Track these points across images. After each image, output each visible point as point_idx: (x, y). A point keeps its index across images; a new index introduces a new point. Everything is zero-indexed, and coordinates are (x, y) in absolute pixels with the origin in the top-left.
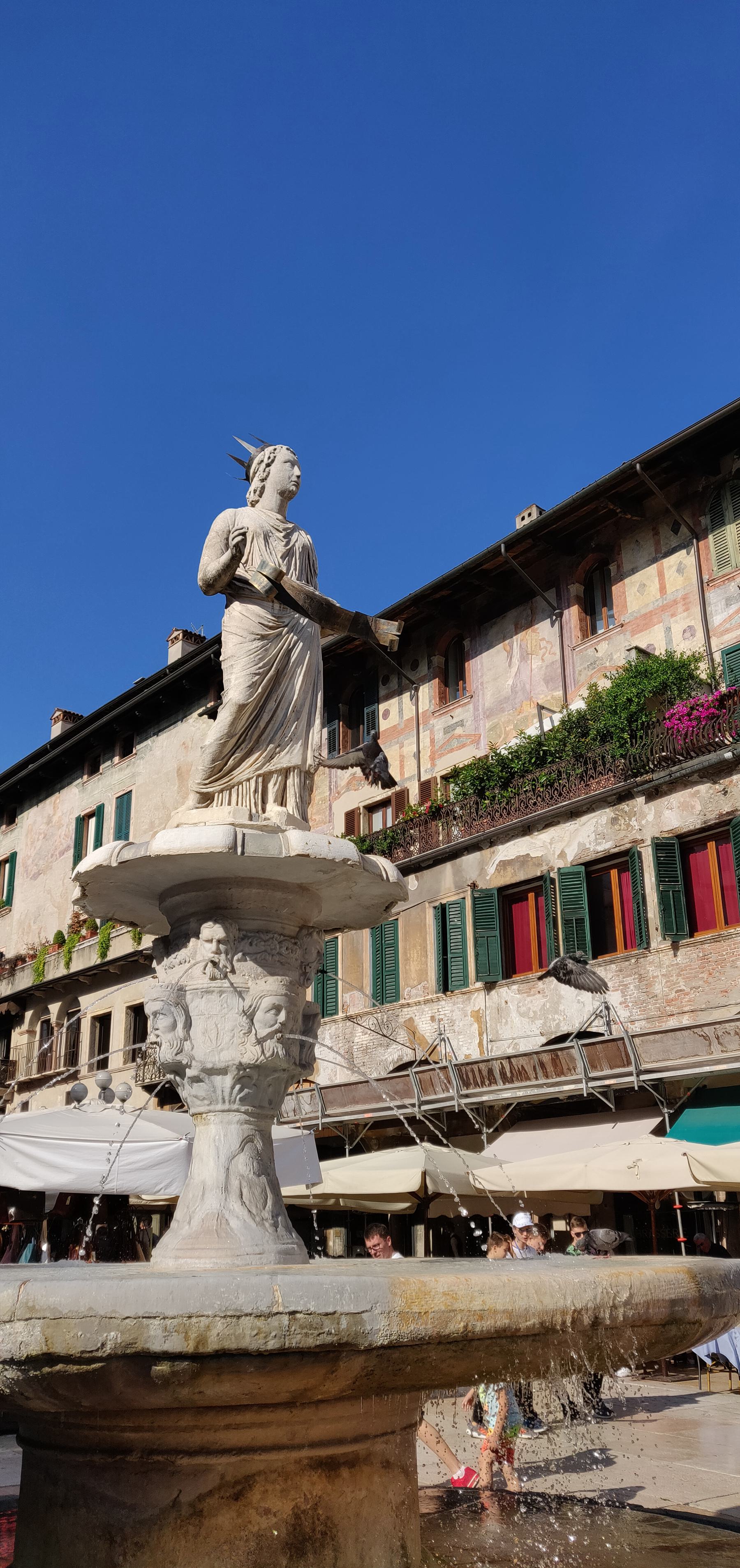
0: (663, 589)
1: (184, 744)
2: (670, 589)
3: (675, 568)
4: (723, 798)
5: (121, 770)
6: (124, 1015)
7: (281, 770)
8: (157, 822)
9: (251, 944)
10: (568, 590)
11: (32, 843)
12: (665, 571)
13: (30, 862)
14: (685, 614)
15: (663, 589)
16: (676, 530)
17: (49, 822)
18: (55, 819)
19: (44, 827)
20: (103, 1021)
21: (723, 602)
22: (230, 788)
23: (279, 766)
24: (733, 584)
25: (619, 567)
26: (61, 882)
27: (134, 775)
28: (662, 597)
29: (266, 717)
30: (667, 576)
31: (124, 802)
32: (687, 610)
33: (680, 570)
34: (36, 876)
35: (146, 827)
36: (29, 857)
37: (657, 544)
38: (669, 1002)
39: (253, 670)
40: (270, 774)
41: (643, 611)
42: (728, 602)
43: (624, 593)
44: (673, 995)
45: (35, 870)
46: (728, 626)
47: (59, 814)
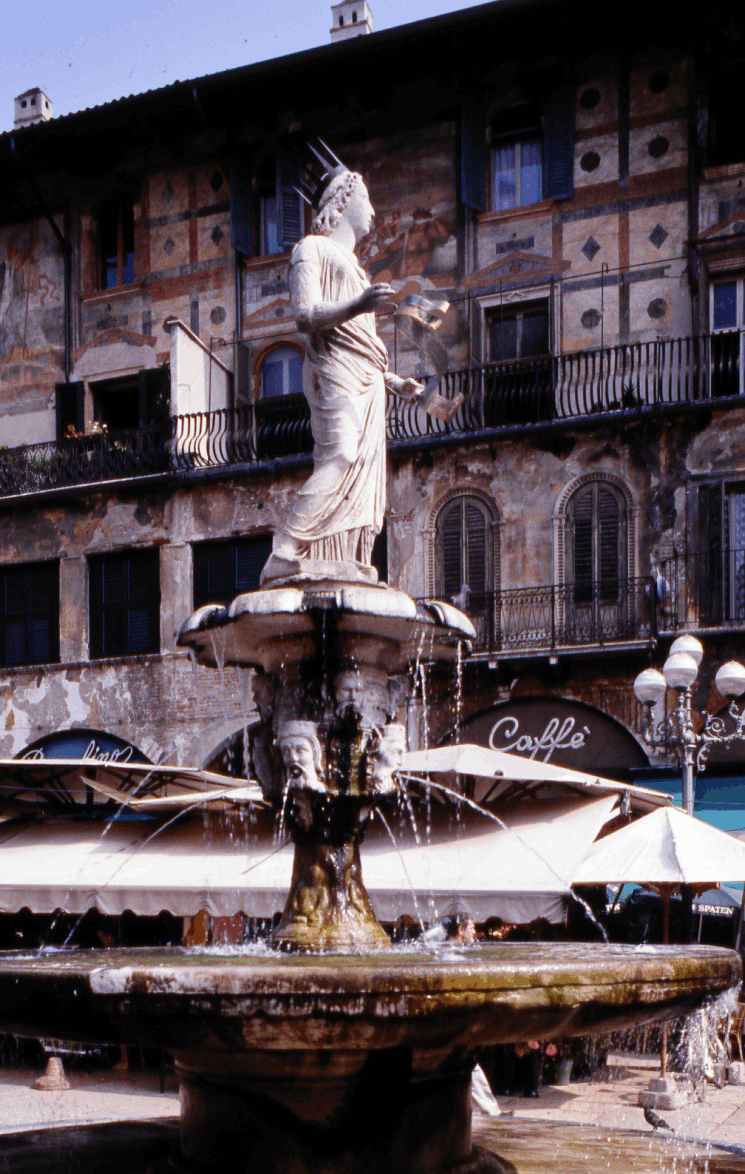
0: (193, 254)
2: (202, 257)
3: (209, 233)
4: (259, 512)
10: (80, 223)
12: (199, 234)
14: (216, 291)
15: (193, 254)
16: (216, 184)
21: (259, 290)
24: (272, 271)
25: (145, 210)
28: (192, 263)
30: (200, 239)
32: (218, 287)
33: (217, 236)
37: (193, 197)
38: (181, 708)
41: (168, 275)
42: (266, 291)
43: (148, 245)
44: (186, 702)
46: (261, 318)
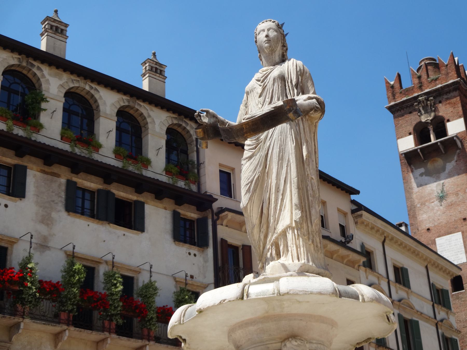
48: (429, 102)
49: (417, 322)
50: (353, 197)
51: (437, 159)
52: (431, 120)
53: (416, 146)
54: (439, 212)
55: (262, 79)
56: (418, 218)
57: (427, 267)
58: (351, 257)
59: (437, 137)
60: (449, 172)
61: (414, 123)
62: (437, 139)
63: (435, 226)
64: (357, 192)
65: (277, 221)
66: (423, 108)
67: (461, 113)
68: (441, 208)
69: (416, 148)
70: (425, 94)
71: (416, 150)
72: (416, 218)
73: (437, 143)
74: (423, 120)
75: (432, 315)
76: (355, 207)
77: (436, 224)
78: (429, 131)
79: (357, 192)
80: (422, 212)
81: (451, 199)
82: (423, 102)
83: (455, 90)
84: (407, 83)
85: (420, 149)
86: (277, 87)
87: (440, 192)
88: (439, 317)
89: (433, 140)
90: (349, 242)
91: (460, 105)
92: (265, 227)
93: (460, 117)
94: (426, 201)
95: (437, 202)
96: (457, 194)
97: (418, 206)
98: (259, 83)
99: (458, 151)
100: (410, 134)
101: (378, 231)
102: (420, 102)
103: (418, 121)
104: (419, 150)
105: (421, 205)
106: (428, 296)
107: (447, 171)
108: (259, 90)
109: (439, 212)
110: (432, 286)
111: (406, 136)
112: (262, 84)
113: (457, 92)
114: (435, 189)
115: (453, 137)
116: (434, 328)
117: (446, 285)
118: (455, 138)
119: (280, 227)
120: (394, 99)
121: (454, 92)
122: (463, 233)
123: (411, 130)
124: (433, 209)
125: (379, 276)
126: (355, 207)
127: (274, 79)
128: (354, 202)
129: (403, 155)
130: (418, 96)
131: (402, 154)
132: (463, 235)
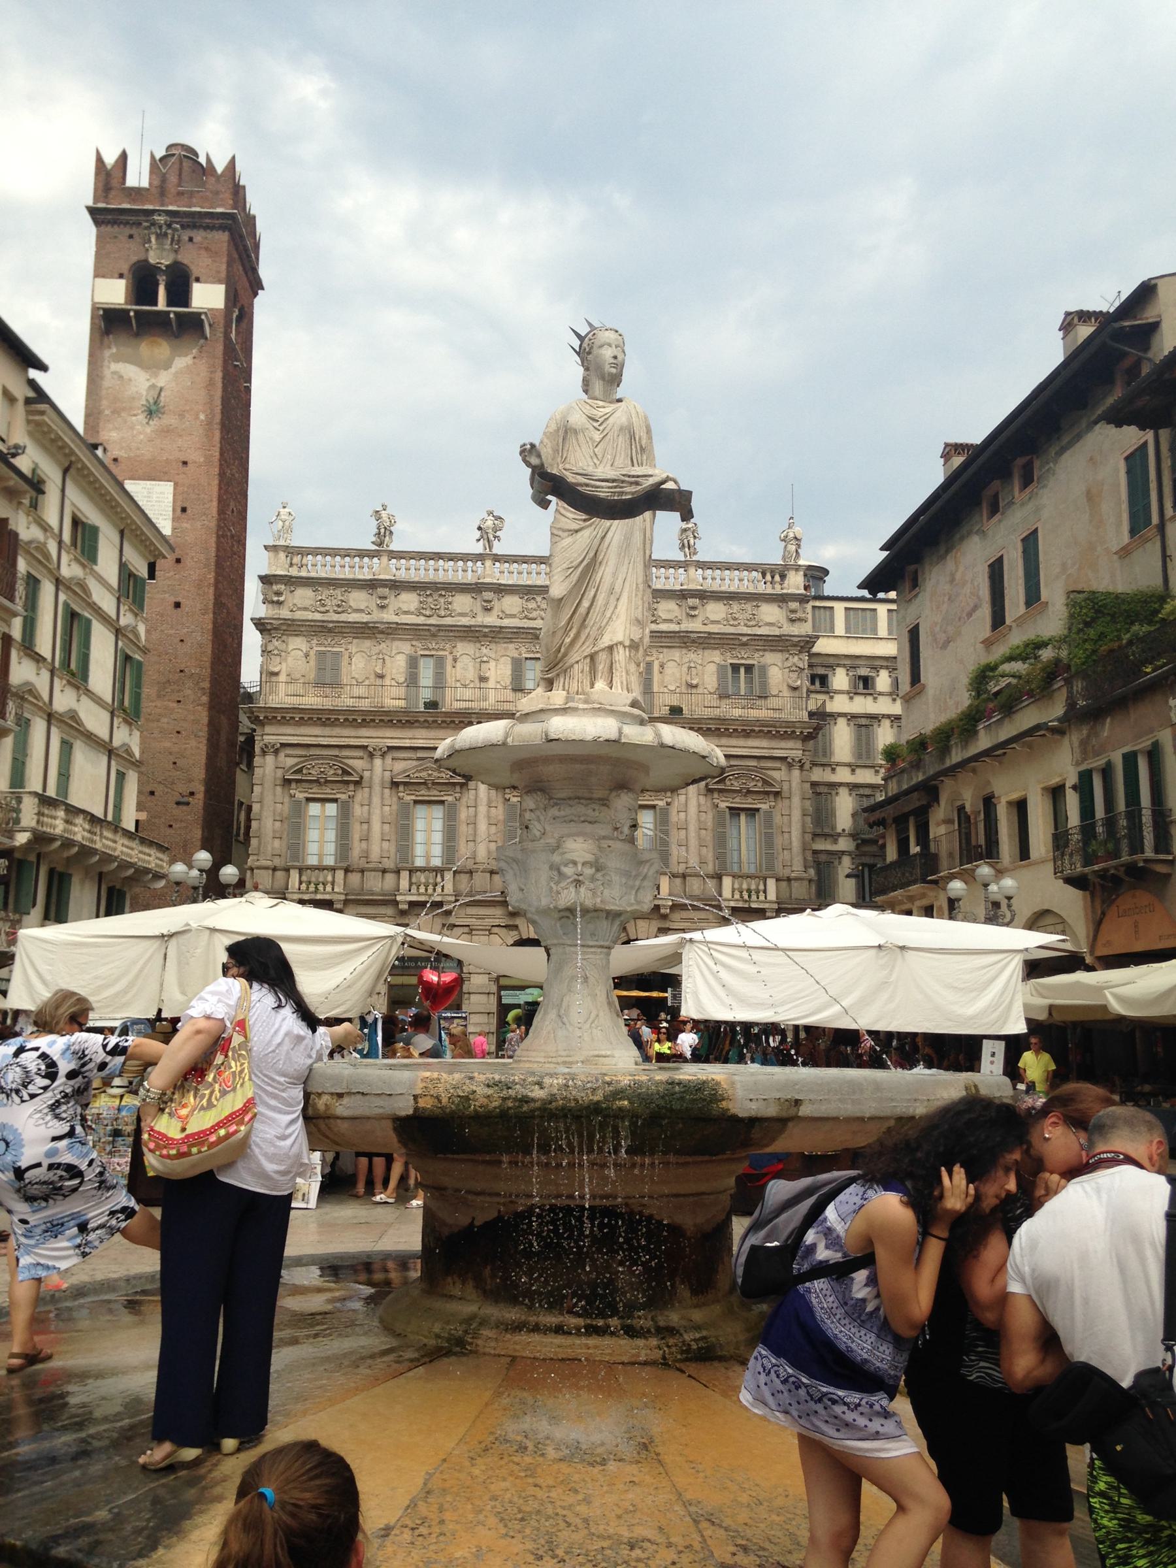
1: (1091, 459)
5: (1023, 505)
6: (1039, 797)
7: (603, 650)
8: (1069, 562)
9: (559, 810)
11: (938, 608)
13: (937, 629)
17: (952, 580)
18: (958, 576)
19: (947, 587)
20: (1021, 807)
22: (565, 671)
23: (602, 646)
26: (972, 649)
27: (1038, 510)
29: (586, 604)
31: (1030, 543)
34: (945, 645)
35: (1058, 570)
36: (936, 624)
39: (565, 566)
40: (596, 653)
45: (942, 637)
47: (961, 569)
48: (169, 231)
49: (89, 622)
50: (33, 373)
51: (160, 340)
52: (167, 266)
53: (126, 303)
54: (142, 437)
55: (601, 420)
56: (101, 433)
57: (122, 533)
58: (11, 483)
59: (170, 303)
60: (176, 372)
61: (134, 259)
62: (168, 305)
63: (129, 458)
64: (43, 367)
65: (601, 631)
66: (158, 236)
67: (223, 275)
68: (148, 430)
69: (129, 307)
70: (168, 213)
71: (129, 311)
72: (98, 432)
73: (168, 313)
74: (152, 261)
75: (113, 615)
76: (31, 394)
77: (132, 455)
78: (157, 285)
79: (43, 367)
80: (111, 426)
81: (169, 420)
82: (160, 227)
83: (222, 228)
84: (138, 176)
85: (136, 312)
86: (622, 441)
87: (152, 401)
88: (123, 622)
89: (162, 305)
90: (14, 455)
91: (225, 260)
92: (574, 631)
93: (220, 282)
94: (124, 409)
95: (142, 417)
96: (181, 416)
97: (107, 412)
98: (596, 424)
99: (202, 341)
100: (121, 276)
101: (61, 448)
102: (153, 224)
103: (142, 257)
104: (132, 314)
105: (113, 412)
106: (114, 581)
107: (173, 370)
108: (597, 436)
109: (142, 437)
110: (123, 566)
111: (112, 277)
112: (601, 428)
113: (227, 233)
114: (144, 393)
115: (200, 314)
116: (113, 638)
117: (143, 572)
118: (203, 317)
119: (606, 641)
120: (106, 197)
121: (220, 232)
122: (176, 485)
123: (125, 268)
124: (132, 428)
125: (45, 527)
126: (31, 394)
127: (621, 429)
128: (32, 384)
129: (101, 312)
130: (153, 212)
131: (99, 308)
132: (175, 489)
